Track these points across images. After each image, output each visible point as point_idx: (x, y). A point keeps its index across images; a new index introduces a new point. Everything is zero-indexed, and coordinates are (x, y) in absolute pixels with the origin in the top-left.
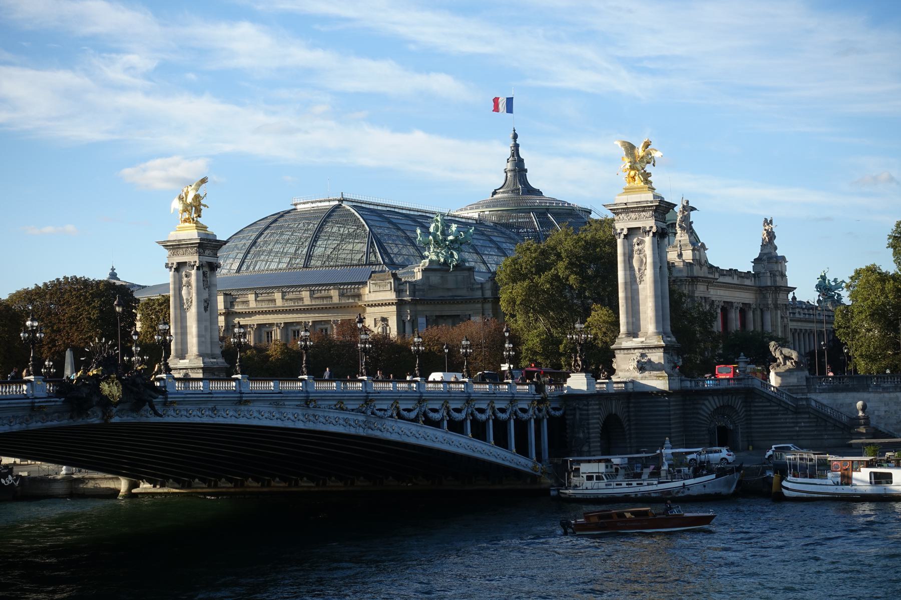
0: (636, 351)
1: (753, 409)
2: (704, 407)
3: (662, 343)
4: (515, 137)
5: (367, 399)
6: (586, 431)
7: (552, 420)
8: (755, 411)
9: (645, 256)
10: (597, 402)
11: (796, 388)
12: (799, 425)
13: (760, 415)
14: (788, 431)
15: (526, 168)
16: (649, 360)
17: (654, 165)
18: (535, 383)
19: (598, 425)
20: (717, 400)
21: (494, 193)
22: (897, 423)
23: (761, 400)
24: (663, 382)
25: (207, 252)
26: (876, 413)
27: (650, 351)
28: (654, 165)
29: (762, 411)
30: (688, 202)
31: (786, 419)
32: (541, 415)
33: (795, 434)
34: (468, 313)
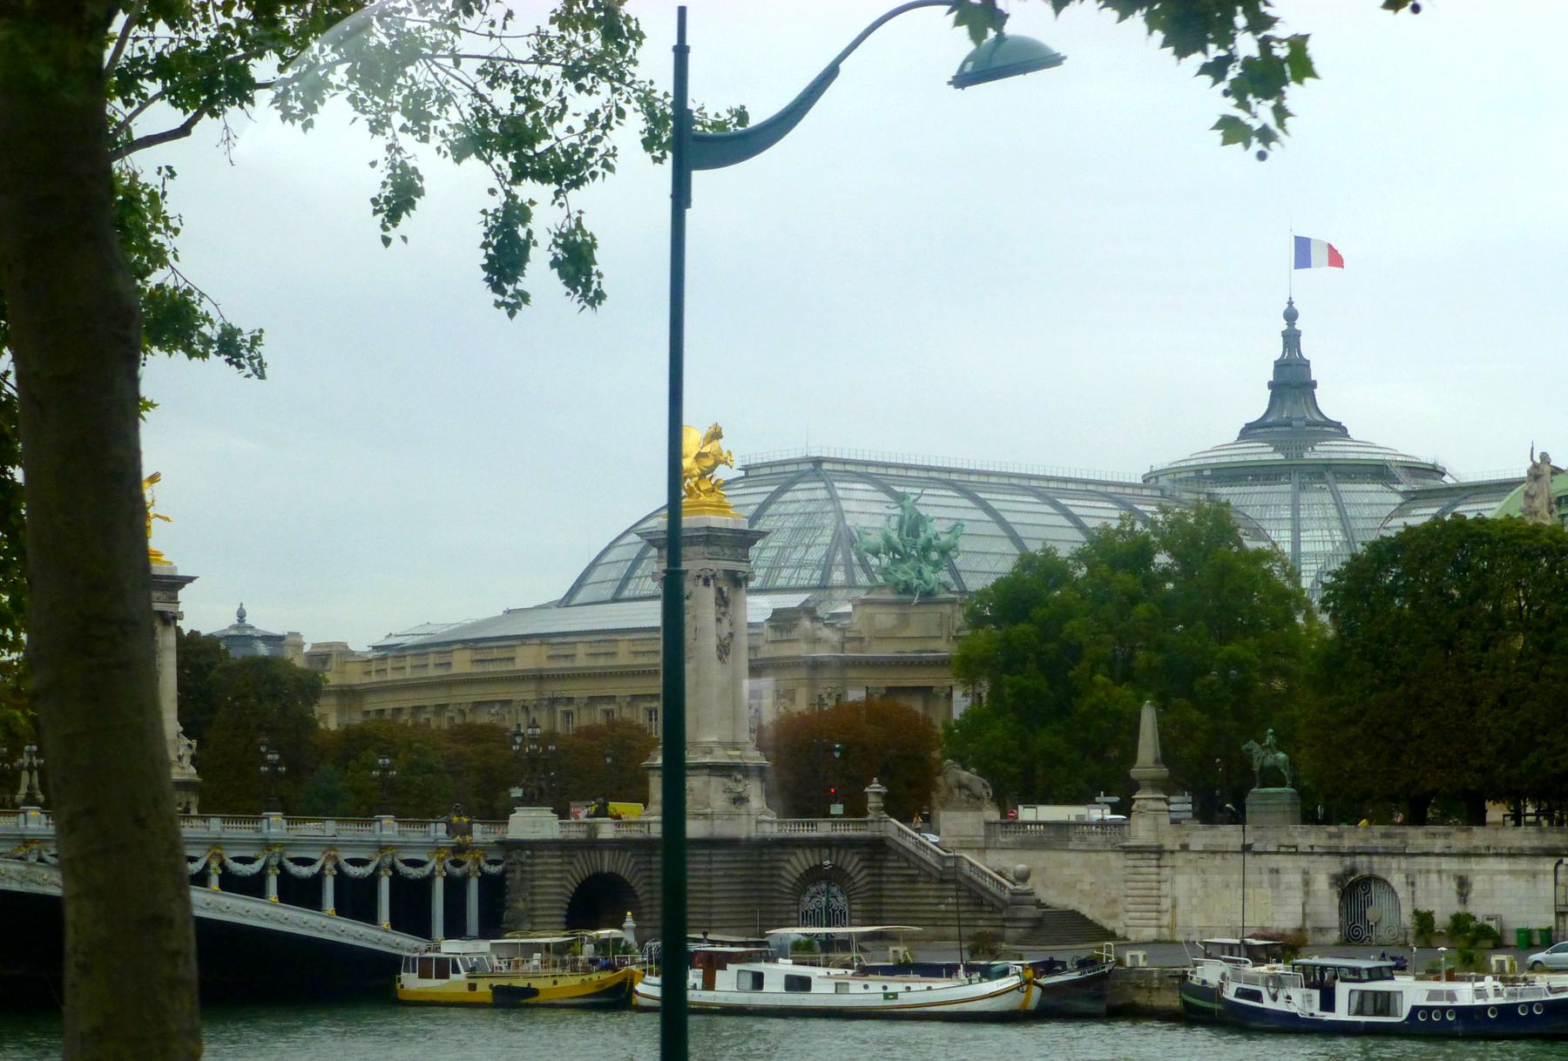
2: (788, 866)
4: (1291, 315)
5: (26, 841)
6: (528, 899)
7: (486, 880)
10: (559, 853)
11: (969, 839)
12: (946, 901)
14: (932, 911)
15: (1313, 379)
18: (449, 824)
19: (559, 890)
20: (809, 856)
22: (1108, 903)
26: (1079, 886)
29: (897, 875)
31: (929, 889)
32: (458, 871)
33: (940, 915)
34: (948, 683)
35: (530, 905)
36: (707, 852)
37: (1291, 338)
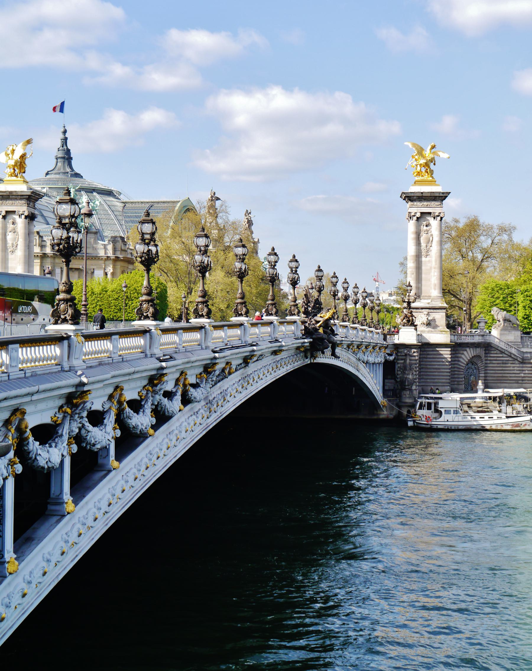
0: (423, 310)
1: (489, 358)
2: (463, 356)
3: (445, 305)
4: (65, 132)
8: (490, 360)
9: (432, 235)
12: (524, 372)
13: (494, 364)
16: (434, 320)
17: (434, 164)
21: (47, 174)
23: (495, 352)
24: (445, 335)
25: (31, 204)
27: (435, 311)
28: (434, 164)
30: (214, 194)
33: (521, 378)
35: (415, 377)
36: (450, 349)
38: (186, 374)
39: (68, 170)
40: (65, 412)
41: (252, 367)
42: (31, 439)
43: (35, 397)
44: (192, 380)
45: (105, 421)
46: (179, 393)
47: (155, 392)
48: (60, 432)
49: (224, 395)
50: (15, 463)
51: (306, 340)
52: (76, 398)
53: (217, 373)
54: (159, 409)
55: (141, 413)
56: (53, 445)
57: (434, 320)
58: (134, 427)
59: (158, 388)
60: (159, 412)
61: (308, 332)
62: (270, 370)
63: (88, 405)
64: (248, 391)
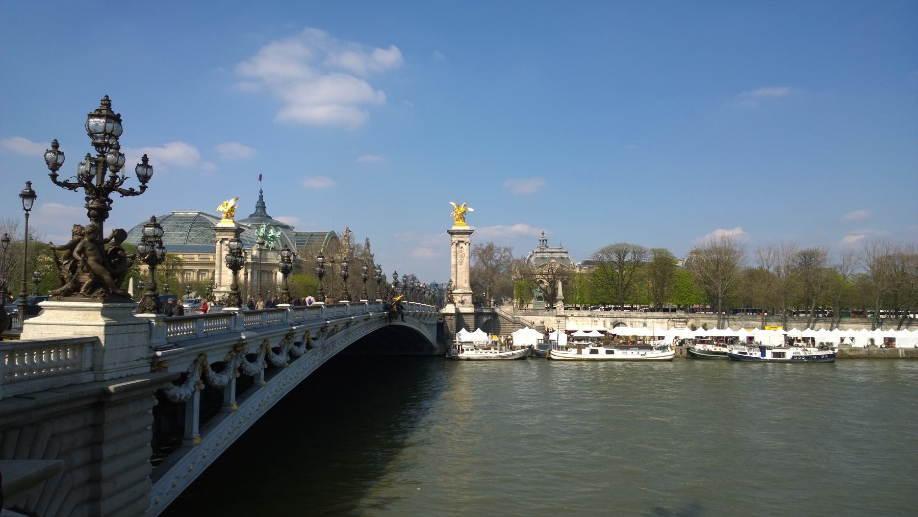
3: (471, 292)
4: (261, 192)
30: (348, 228)
37: (261, 197)
38: (309, 333)
39: (264, 214)
40: (232, 355)
41: (351, 328)
42: (210, 370)
43: (212, 347)
44: (313, 335)
45: (258, 359)
46: (305, 343)
47: (289, 343)
48: (229, 366)
49: (333, 343)
50: (200, 384)
51: (385, 313)
52: (239, 347)
53: (328, 331)
54: (292, 352)
55: (280, 354)
56: (224, 373)
57: (465, 300)
58: (275, 362)
59: (291, 340)
60: (292, 354)
61: (386, 308)
62: (363, 329)
63: (246, 351)
64: (350, 340)
